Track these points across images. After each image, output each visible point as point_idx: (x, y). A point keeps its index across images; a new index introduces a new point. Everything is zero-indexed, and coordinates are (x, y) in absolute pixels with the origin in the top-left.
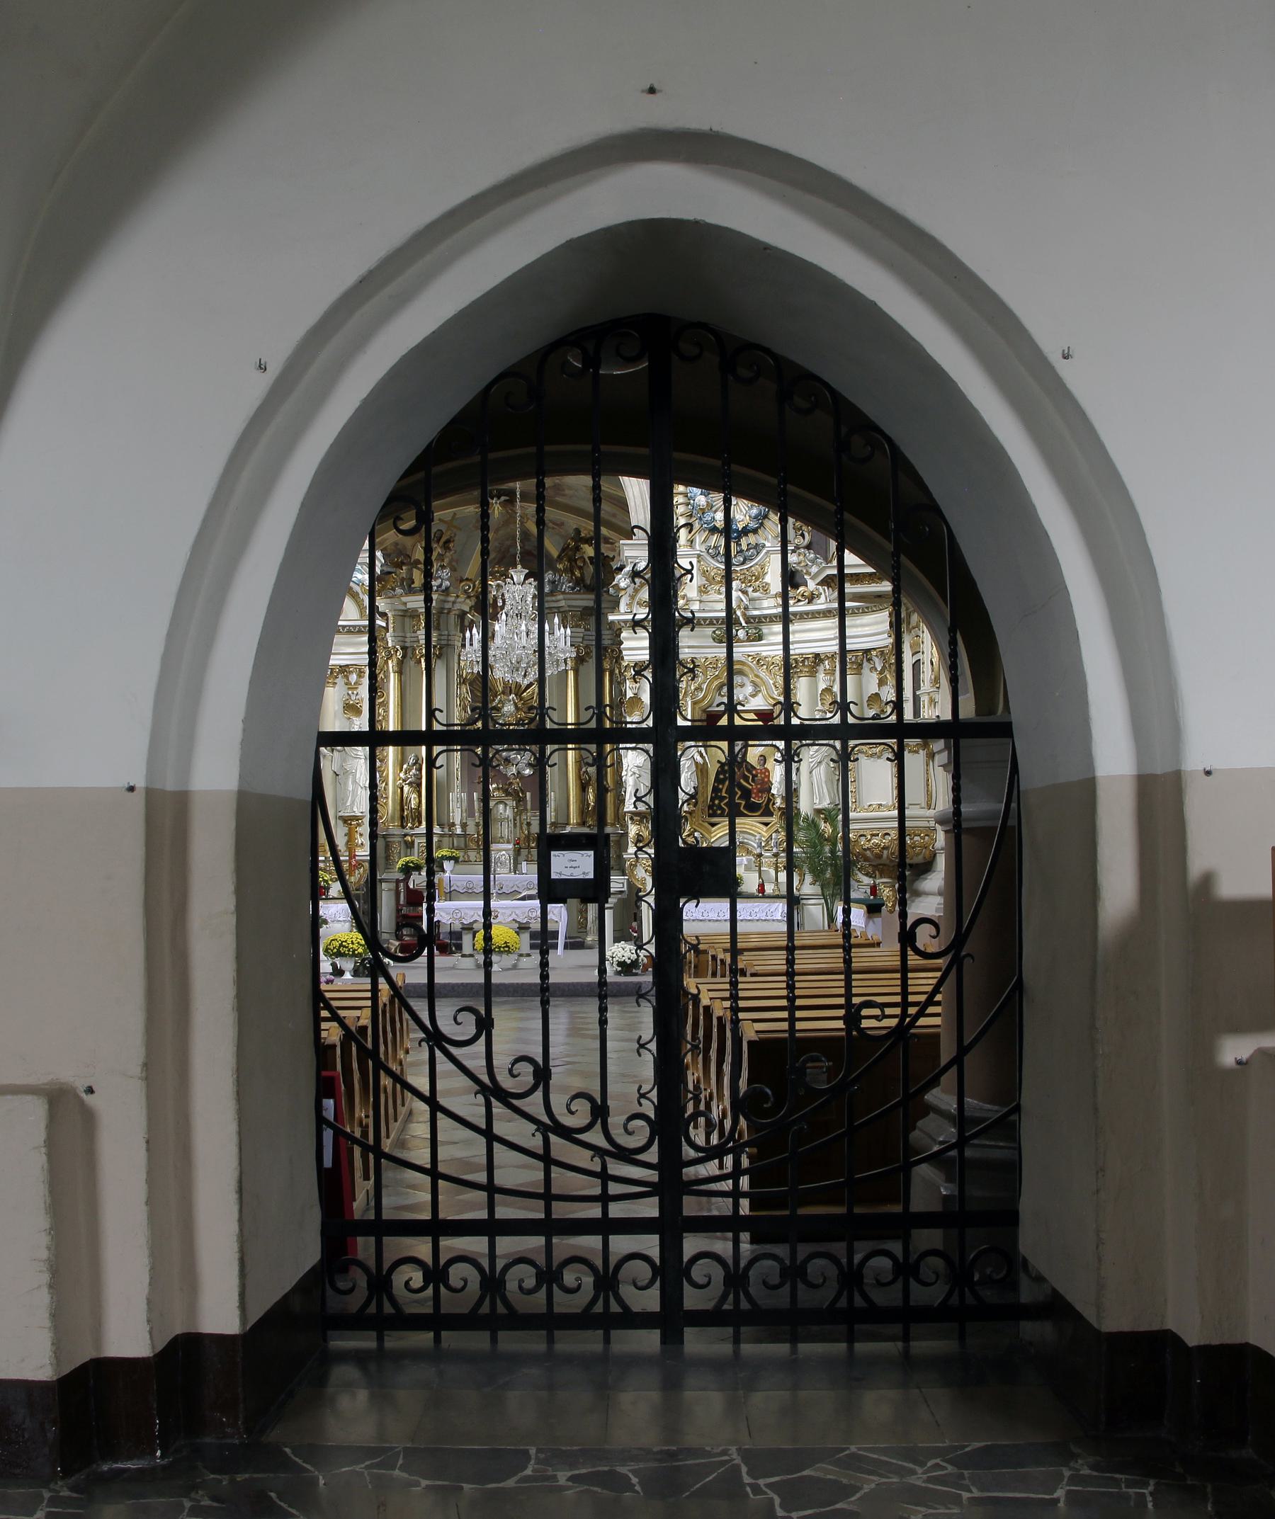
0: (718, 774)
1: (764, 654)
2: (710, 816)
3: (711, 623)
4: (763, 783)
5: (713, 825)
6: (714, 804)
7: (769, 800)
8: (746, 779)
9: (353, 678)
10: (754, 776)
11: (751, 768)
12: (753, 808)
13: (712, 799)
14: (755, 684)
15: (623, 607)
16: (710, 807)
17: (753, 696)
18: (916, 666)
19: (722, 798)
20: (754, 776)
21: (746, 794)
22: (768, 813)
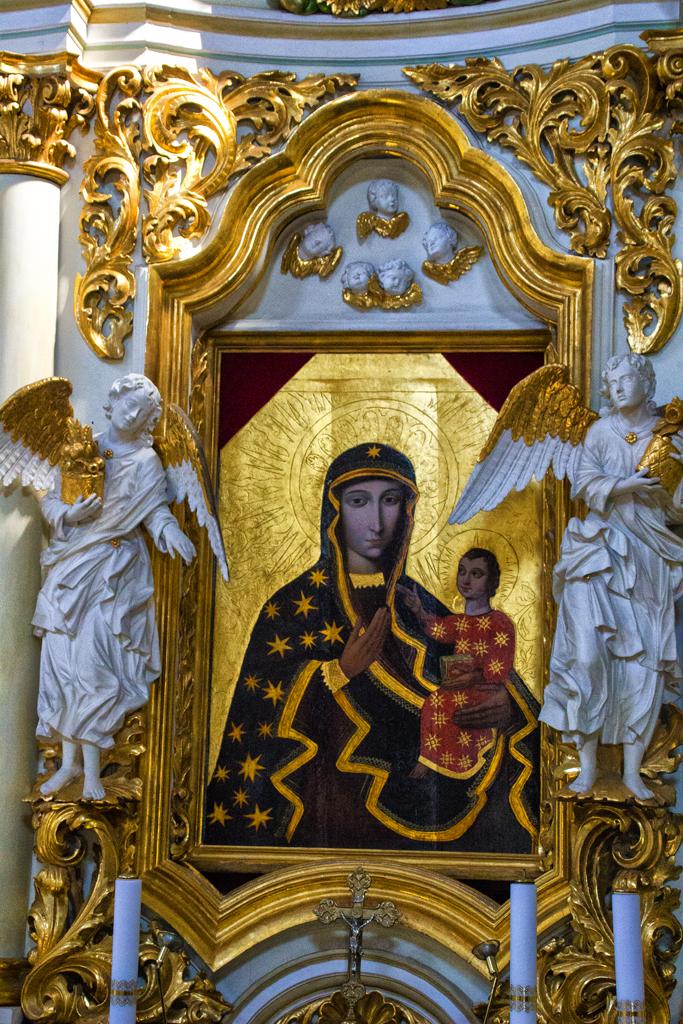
0: (264, 630)
1: (513, 62)
2: (215, 835)
5: (228, 881)
6: (237, 781)
7: (509, 768)
8: (397, 659)
10: (440, 649)
11: (419, 608)
12: (428, 802)
13: (231, 754)
14: (455, 215)
16: (217, 793)
17: (444, 272)
20: (447, 647)
21: (397, 734)
22: (497, 833)
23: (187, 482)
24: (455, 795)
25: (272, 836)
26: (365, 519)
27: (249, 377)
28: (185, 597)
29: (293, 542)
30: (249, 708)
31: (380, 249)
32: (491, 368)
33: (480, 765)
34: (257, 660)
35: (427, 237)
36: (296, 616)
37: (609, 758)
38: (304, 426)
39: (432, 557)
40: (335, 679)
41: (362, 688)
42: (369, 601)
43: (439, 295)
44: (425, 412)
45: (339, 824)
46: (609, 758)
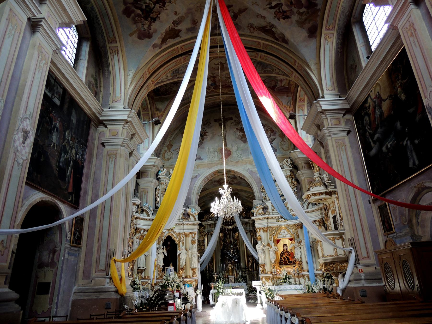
3: (276, 218)
4: (292, 256)
8: (288, 255)
9: (193, 235)
11: (288, 252)
12: (291, 262)
15: (255, 215)
16: (280, 263)
18: (334, 218)
19: (282, 260)
21: (288, 259)
22: (294, 264)
23: (276, 247)
24: (291, 262)
25: (283, 265)
26: (285, 248)
27: (278, 241)
28: (276, 253)
29: (282, 250)
30: (281, 258)
31: (284, 233)
32: (291, 240)
33: (292, 260)
34: (281, 256)
35: (286, 233)
36: (282, 253)
37: (298, 259)
38: (281, 243)
39: (289, 250)
40: (285, 256)
41: (286, 257)
42: (286, 252)
43: (287, 236)
44: (287, 242)
45: (286, 264)
46: (298, 259)
